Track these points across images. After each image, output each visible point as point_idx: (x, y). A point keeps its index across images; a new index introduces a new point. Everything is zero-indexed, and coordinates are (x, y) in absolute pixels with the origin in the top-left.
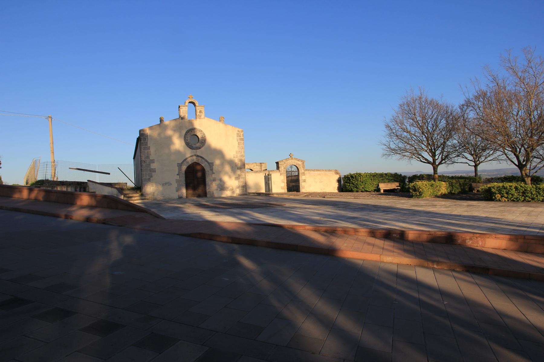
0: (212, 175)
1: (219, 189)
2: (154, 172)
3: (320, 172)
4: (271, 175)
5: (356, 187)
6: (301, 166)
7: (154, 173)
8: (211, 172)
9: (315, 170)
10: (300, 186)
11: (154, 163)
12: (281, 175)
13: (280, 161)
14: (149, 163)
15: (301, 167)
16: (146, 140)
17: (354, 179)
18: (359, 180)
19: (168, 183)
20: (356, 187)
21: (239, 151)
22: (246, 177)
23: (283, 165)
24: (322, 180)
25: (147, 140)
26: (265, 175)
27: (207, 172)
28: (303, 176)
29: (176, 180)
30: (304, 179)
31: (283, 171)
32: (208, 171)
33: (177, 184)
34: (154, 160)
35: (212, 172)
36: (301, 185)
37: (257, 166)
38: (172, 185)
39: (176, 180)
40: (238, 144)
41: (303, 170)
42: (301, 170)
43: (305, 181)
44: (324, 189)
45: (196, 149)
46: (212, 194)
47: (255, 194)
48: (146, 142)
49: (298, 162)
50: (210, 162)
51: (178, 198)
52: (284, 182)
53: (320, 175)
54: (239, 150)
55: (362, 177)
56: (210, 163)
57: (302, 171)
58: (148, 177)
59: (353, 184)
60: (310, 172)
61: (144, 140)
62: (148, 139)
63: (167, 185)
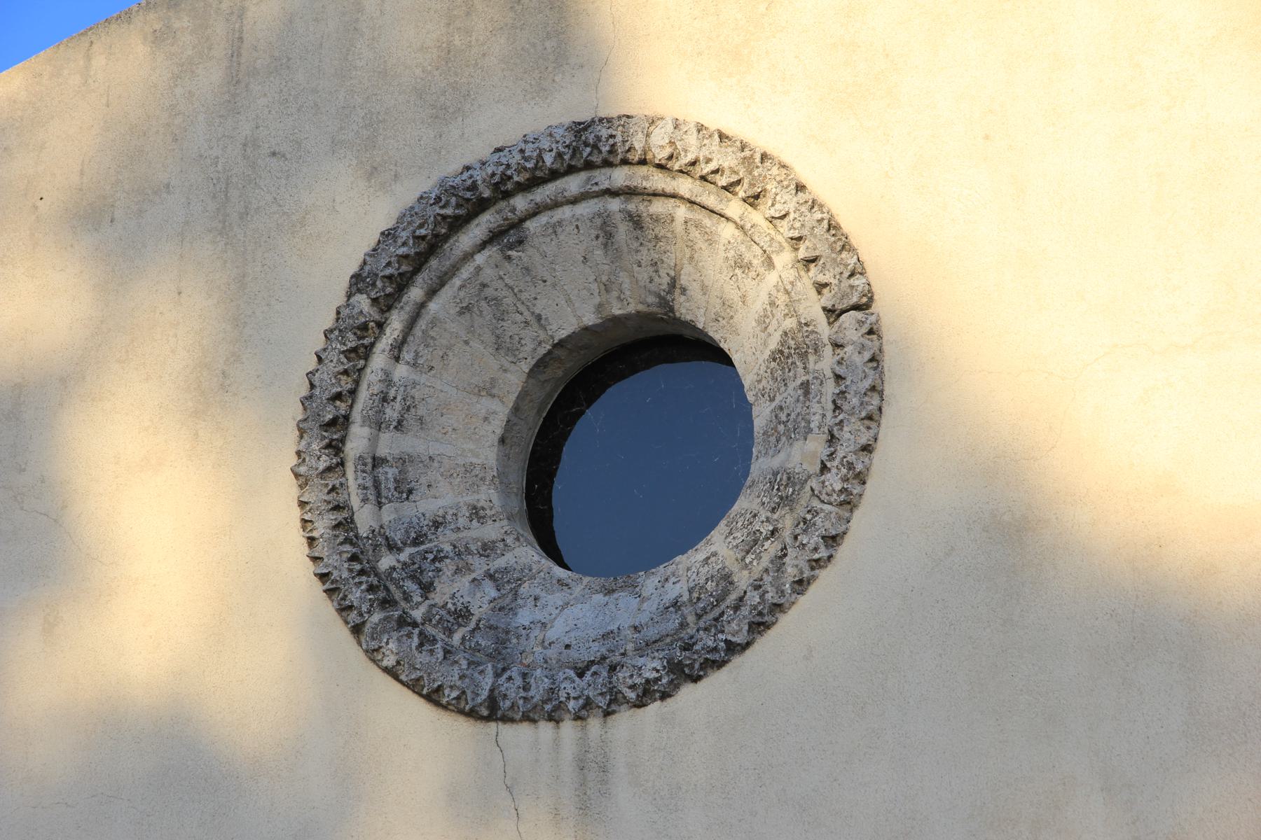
45: (591, 686)
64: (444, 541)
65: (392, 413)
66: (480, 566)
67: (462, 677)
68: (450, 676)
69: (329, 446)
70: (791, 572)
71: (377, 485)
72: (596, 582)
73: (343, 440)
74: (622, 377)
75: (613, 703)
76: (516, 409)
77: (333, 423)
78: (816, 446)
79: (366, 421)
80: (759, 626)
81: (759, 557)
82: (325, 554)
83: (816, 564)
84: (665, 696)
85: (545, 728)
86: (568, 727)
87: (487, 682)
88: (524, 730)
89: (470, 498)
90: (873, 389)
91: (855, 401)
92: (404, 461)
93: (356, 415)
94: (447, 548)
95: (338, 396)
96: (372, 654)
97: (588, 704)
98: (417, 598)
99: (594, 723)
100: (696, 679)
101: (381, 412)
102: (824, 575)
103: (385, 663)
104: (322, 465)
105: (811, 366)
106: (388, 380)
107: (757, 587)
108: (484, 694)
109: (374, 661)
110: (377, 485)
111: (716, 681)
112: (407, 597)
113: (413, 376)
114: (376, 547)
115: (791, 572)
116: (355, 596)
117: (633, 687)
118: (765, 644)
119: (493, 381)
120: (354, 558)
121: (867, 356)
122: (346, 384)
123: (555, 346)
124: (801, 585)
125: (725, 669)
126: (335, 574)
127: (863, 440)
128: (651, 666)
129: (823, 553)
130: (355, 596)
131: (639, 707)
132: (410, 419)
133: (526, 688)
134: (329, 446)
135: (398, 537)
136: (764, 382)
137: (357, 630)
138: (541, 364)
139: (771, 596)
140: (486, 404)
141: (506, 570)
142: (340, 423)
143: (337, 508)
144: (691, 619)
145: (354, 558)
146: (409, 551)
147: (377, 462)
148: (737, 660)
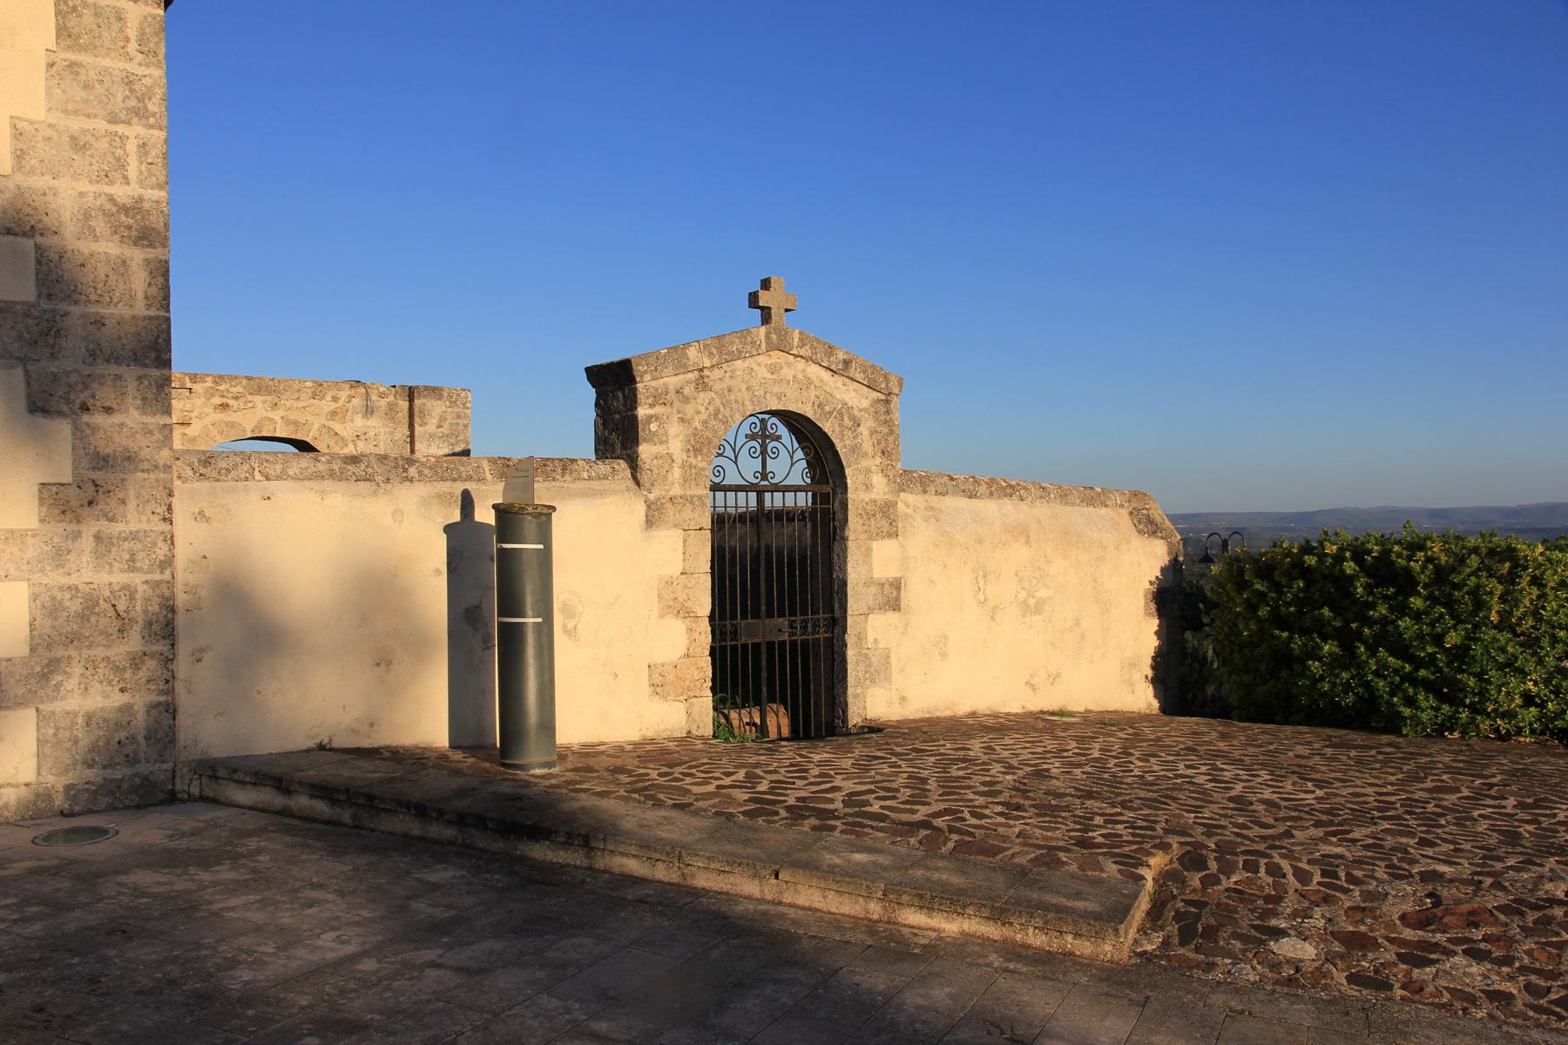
3: (1023, 506)
4: (544, 516)
5: (1429, 686)
6: (864, 430)
9: (983, 489)
10: (851, 653)
12: (650, 523)
13: (647, 356)
15: (867, 446)
17: (1417, 603)
18: (1494, 617)
20: (1447, 691)
21: (78, 144)
23: (686, 400)
24: (1043, 593)
26: (456, 516)
28: (875, 545)
30: (892, 573)
31: (677, 472)
36: (861, 638)
37: (369, 411)
41: (878, 480)
42: (868, 471)
43: (892, 597)
44: (1055, 678)
47: (303, 802)
49: (839, 380)
52: (684, 613)
53: (1021, 532)
54: (77, 125)
55: (1536, 581)
57: (868, 487)
59: (1401, 649)
60: (934, 500)
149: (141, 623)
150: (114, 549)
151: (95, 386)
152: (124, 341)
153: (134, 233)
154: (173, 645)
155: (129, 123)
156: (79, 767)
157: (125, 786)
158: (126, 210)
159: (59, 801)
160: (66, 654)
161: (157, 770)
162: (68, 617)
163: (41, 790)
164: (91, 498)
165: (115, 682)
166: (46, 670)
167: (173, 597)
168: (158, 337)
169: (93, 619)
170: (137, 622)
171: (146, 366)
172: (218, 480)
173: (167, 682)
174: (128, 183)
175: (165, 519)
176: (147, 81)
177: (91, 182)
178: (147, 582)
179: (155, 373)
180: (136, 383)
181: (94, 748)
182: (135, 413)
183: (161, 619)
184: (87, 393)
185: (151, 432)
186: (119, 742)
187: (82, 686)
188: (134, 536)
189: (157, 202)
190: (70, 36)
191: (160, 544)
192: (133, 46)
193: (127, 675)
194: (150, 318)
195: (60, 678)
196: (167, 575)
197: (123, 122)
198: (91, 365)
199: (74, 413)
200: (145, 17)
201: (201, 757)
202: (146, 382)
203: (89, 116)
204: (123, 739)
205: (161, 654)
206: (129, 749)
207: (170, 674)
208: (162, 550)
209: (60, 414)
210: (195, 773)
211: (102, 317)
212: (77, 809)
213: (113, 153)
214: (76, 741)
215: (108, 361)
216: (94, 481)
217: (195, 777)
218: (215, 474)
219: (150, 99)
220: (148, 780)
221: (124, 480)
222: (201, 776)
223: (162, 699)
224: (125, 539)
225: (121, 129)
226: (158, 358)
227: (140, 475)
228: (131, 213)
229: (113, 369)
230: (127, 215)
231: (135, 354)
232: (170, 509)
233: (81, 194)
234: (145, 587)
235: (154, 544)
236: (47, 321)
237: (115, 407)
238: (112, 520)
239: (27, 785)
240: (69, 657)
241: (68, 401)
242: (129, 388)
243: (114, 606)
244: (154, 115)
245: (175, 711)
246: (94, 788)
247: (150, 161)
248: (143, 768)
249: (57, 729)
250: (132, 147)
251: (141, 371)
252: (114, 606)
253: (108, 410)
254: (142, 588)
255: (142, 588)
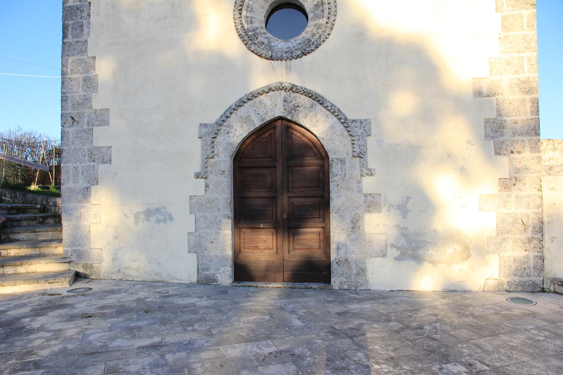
0: (359, 182)
1: (393, 252)
2: (104, 163)
7: (105, 165)
8: (358, 165)
11: (105, 122)
14: (88, 123)
16: (82, 30)
19: (158, 210)
21: (508, 63)
22: (546, 193)
25: (86, 31)
27: (335, 169)
29: (191, 197)
32: (343, 161)
33: (193, 216)
34: (109, 109)
35: (363, 165)
37: (554, 149)
38: (171, 219)
39: (191, 197)
40: (504, 27)
45: (288, 55)
46: (358, 274)
48: (82, 39)
50: (350, 116)
51: (194, 279)
56: (353, 121)
58: (82, 184)
61: (79, 30)
62: (89, 28)
63: (153, 219)
64: (258, 31)
65: (249, 9)
66: (264, 36)
67: (266, 52)
68: (264, 52)
69: (239, 14)
70: (322, 39)
71: (247, 21)
72: (282, 40)
73: (241, 13)
74: (281, 9)
75: (291, 59)
76: (266, 12)
77: (240, 10)
78: (325, 20)
79: (245, 10)
80: (317, 47)
81: (316, 37)
82: (240, 31)
83: (326, 38)
84: (301, 57)
85: (280, 62)
86: (284, 62)
87: (270, 54)
88: (276, 62)
89: (261, 25)
90: (335, 11)
91: (333, 13)
92: (251, 17)
93: (244, 9)
94: (259, 33)
95: (241, 5)
96: (249, 48)
97: (288, 58)
98: (256, 40)
99: (288, 61)
100: (306, 55)
101: (247, 9)
102: (327, 40)
103: (252, 50)
104: (239, 17)
105: (324, 7)
106: (248, 4)
107: (316, 41)
108: (270, 55)
109: (249, 49)
110: (247, 21)
111: (309, 56)
112: (254, 39)
113: (253, 4)
114: (248, 31)
115: (322, 39)
116: (246, 38)
117: (295, 56)
118: (317, 50)
119: (264, 6)
120: (245, 32)
121: (335, 5)
122: (242, 4)
123: (274, 2)
124: (324, 41)
125: (310, 54)
126: (242, 35)
127: (334, 19)
128: (299, 53)
129: (327, 36)
130: (246, 38)
131: (296, 59)
132: (252, 11)
133: (277, 55)
134: (239, 14)
135: (251, 30)
136: (312, 10)
137: (246, 44)
138: (271, 5)
139: (319, 43)
140: (262, 10)
141: (268, 37)
142: (241, 10)
143: (242, 24)
144: (304, 46)
145: (245, 32)
146: (253, 32)
147: (247, 17)
148: (313, 53)
149: (531, 227)
150: (522, 201)
151: (515, 144)
152: (524, 128)
153: (527, 90)
154: (542, 235)
155: (524, 52)
156: (512, 275)
157: (527, 284)
158: (524, 82)
159: (506, 287)
160: (507, 236)
161: (538, 280)
162: (508, 224)
163: (500, 282)
164: (514, 183)
165: (523, 247)
166: (501, 242)
167: (543, 218)
168: (535, 125)
169: (516, 225)
170: (530, 227)
171: (531, 136)
172: (555, 176)
173: (541, 248)
174: (524, 73)
175: (539, 190)
176: (530, 36)
177: (512, 75)
178: (533, 212)
179: (535, 138)
180: (529, 142)
181: (516, 269)
182: (528, 153)
183: (538, 226)
184: (513, 147)
185: (533, 159)
186: (524, 268)
187: (512, 248)
188: (529, 196)
189: (535, 78)
190: (505, 27)
191: (538, 199)
192: (526, 25)
193: (527, 245)
194: (533, 119)
195: (505, 245)
196: (540, 210)
197: (522, 52)
198: (514, 137)
199: (509, 154)
200: (530, 14)
201: (553, 277)
202: (532, 142)
203: (511, 53)
204: (526, 267)
205: (538, 238)
206: (528, 271)
207: (542, 246)
208: (538, 201)
209: (504, 154)
210: (552, 283)
211: (517, 120)
212: (511, 290)
213: (519, 63)
214: (511, 267)
215: (519, 135)
216: (515, 177)
217: (552, 284)
218: (554, 173)
219: (531, 42)
220: (534, 283)
221: (525, 176)
222: (554, 284)
223: (539, 254)
224: (526, 197)
225: (522, 55)
226: (536, 133)
227: (531, 175)
228: (526, 83)
229: (521, 138)
230: (524, 84)
231: (528, 132)
232: (541, 186)
233: (509, 80)
234: (533, 214)
235: (536, 199)
236: (500, 124)
237: (522, 151)
238: (521, 191)
239: (496, 280)
240: (508, 238)
241: (507, 150)
242: (526, 144)
243: (522, 221)
244: (533, 47)
245: (543, 259)
246: (516, 283)
247: (531, 64)
248: (533, 278)
249: (505, 262)
250: (525, 60)
251: (530, 138)
252: (522, 221)
253: (519, 152)
254: (532, 215)
255: (532, 215)
